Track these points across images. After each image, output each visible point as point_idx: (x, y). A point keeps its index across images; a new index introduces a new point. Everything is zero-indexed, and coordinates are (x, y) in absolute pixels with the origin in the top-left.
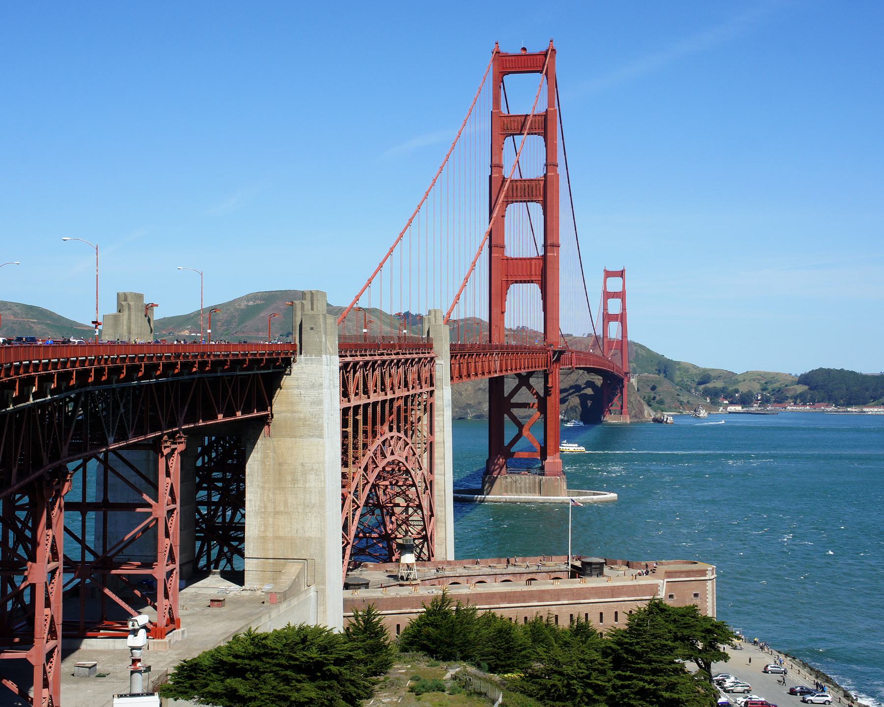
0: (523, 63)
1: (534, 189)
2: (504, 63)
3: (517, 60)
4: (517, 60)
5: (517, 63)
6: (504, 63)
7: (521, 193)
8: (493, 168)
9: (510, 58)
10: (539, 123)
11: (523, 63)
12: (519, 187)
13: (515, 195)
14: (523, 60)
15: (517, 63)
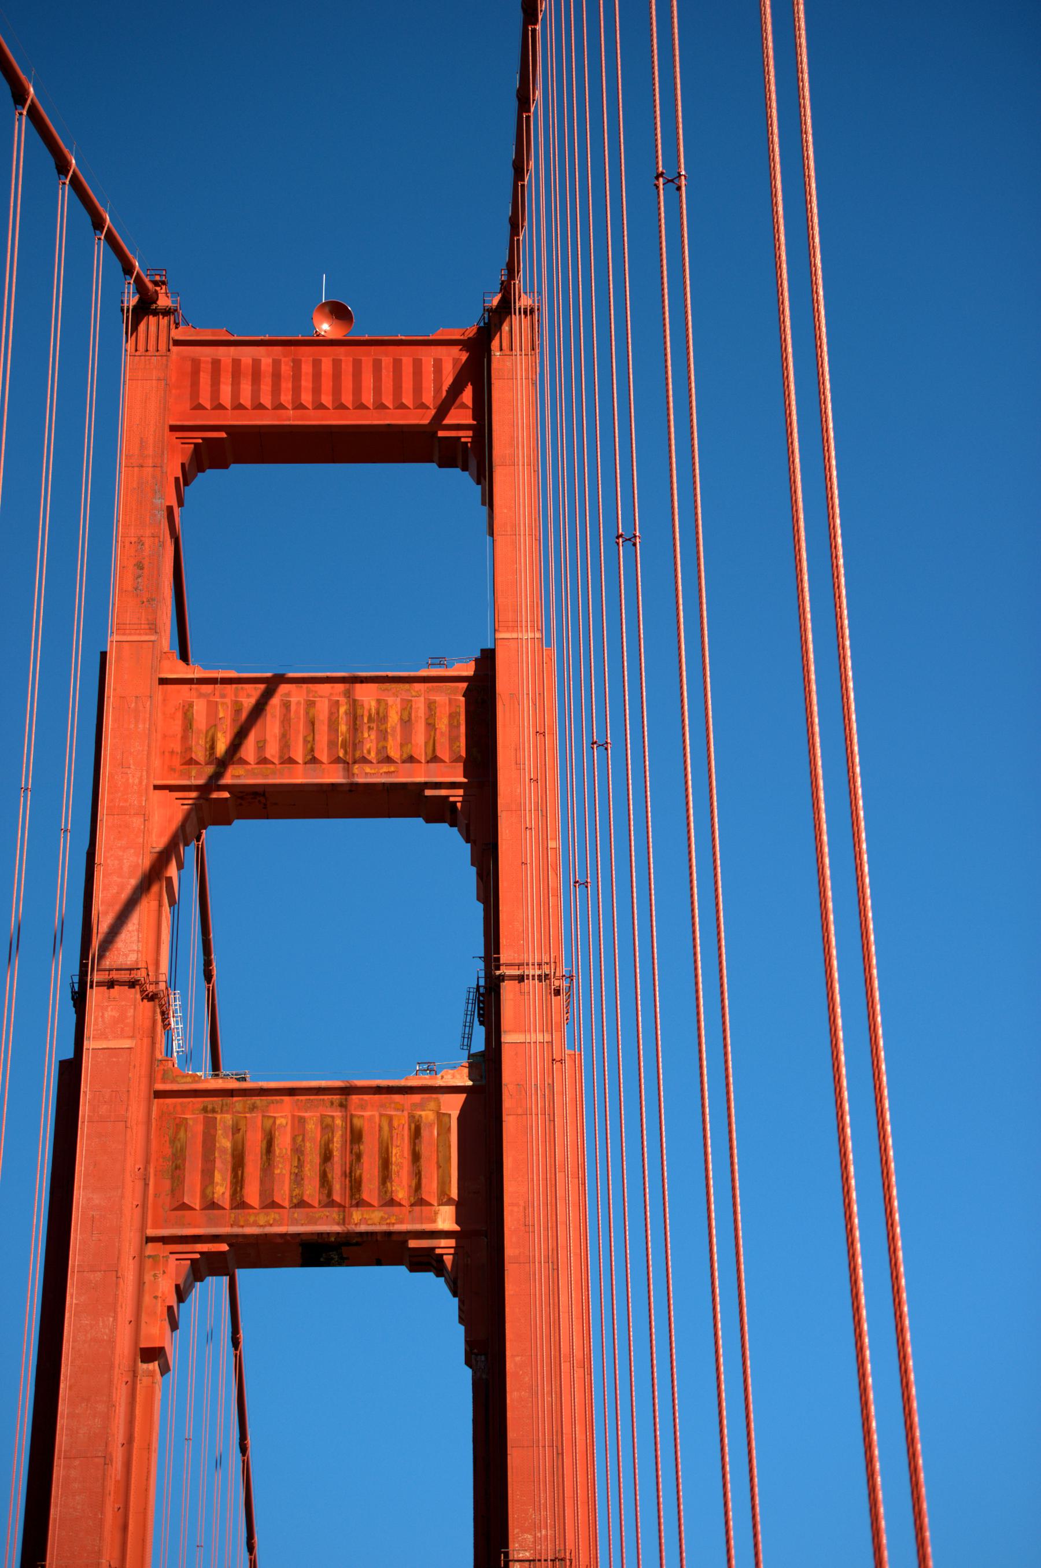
0: (327, 384)
1: (400, 1155)
2: (205, 379)
3: (286, 369)
4: (286, 369)
5: (287, 385)
6: (205, 379)
7: (298, 1178)
8: (94, 996)
9: (247, 355)
10: (430, 726)
11: (327, 384)
12: (283, 1144)
13: (252, 1194)
14: (327, 366)
15: (287, 385)
